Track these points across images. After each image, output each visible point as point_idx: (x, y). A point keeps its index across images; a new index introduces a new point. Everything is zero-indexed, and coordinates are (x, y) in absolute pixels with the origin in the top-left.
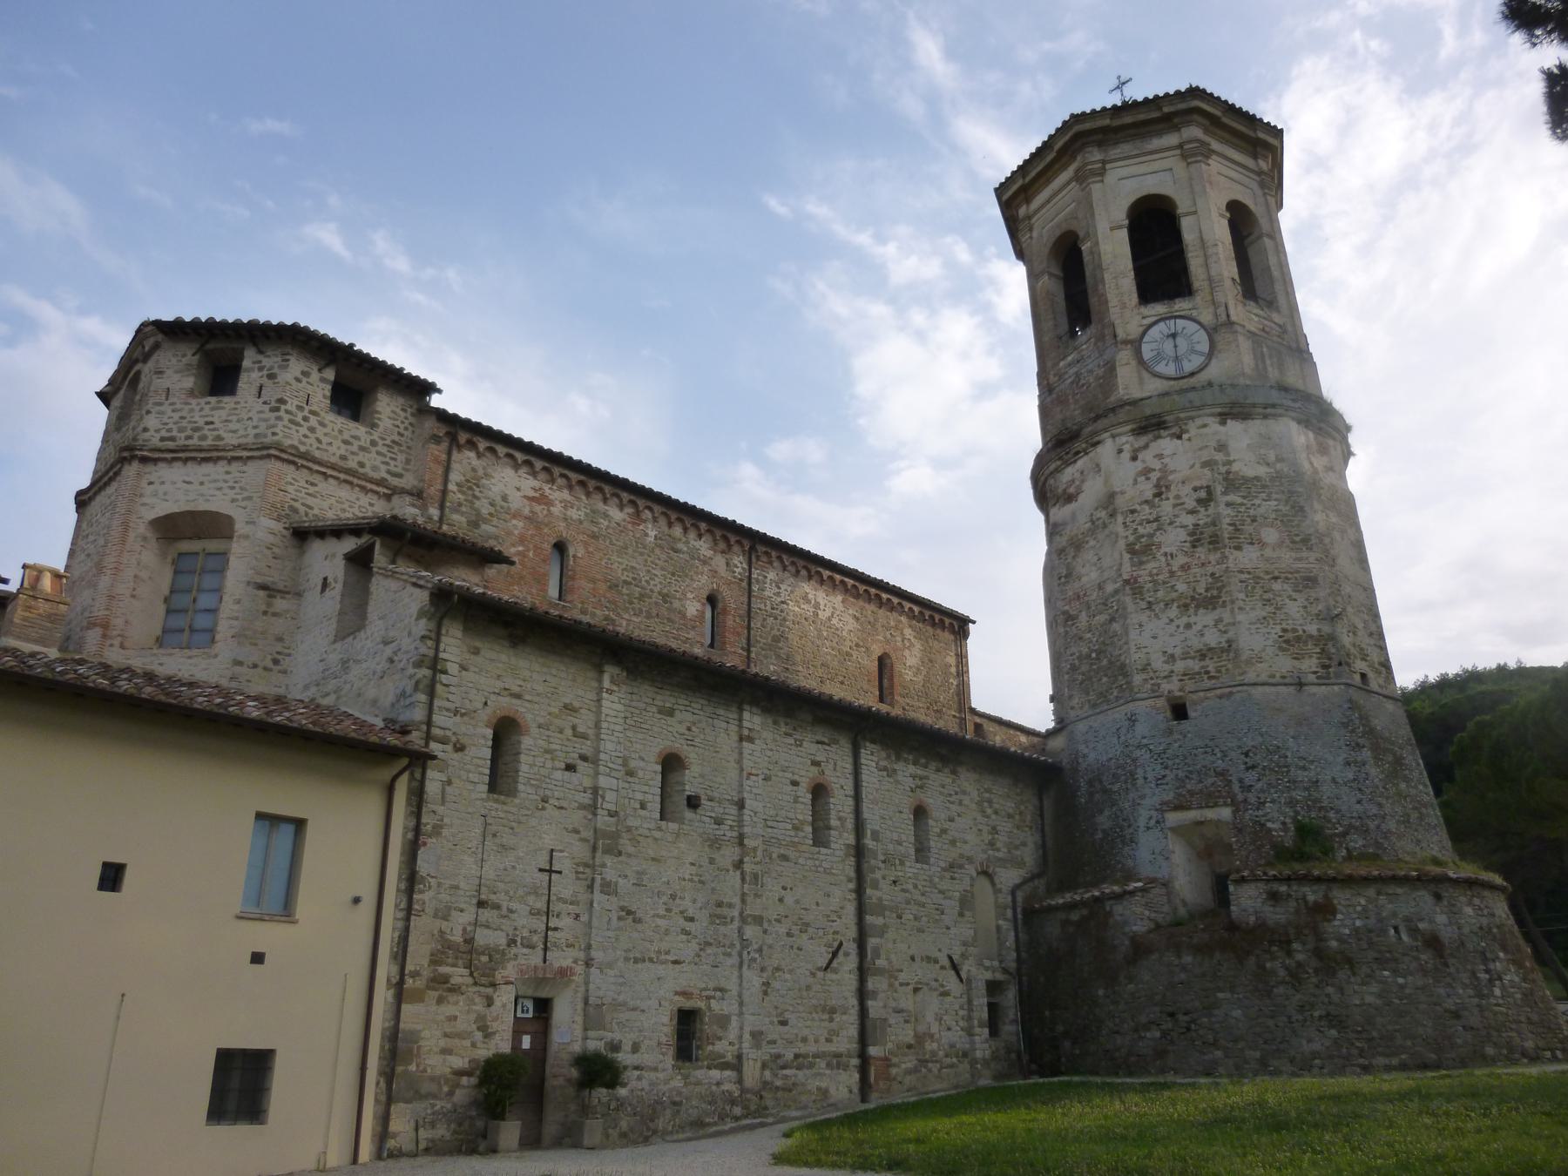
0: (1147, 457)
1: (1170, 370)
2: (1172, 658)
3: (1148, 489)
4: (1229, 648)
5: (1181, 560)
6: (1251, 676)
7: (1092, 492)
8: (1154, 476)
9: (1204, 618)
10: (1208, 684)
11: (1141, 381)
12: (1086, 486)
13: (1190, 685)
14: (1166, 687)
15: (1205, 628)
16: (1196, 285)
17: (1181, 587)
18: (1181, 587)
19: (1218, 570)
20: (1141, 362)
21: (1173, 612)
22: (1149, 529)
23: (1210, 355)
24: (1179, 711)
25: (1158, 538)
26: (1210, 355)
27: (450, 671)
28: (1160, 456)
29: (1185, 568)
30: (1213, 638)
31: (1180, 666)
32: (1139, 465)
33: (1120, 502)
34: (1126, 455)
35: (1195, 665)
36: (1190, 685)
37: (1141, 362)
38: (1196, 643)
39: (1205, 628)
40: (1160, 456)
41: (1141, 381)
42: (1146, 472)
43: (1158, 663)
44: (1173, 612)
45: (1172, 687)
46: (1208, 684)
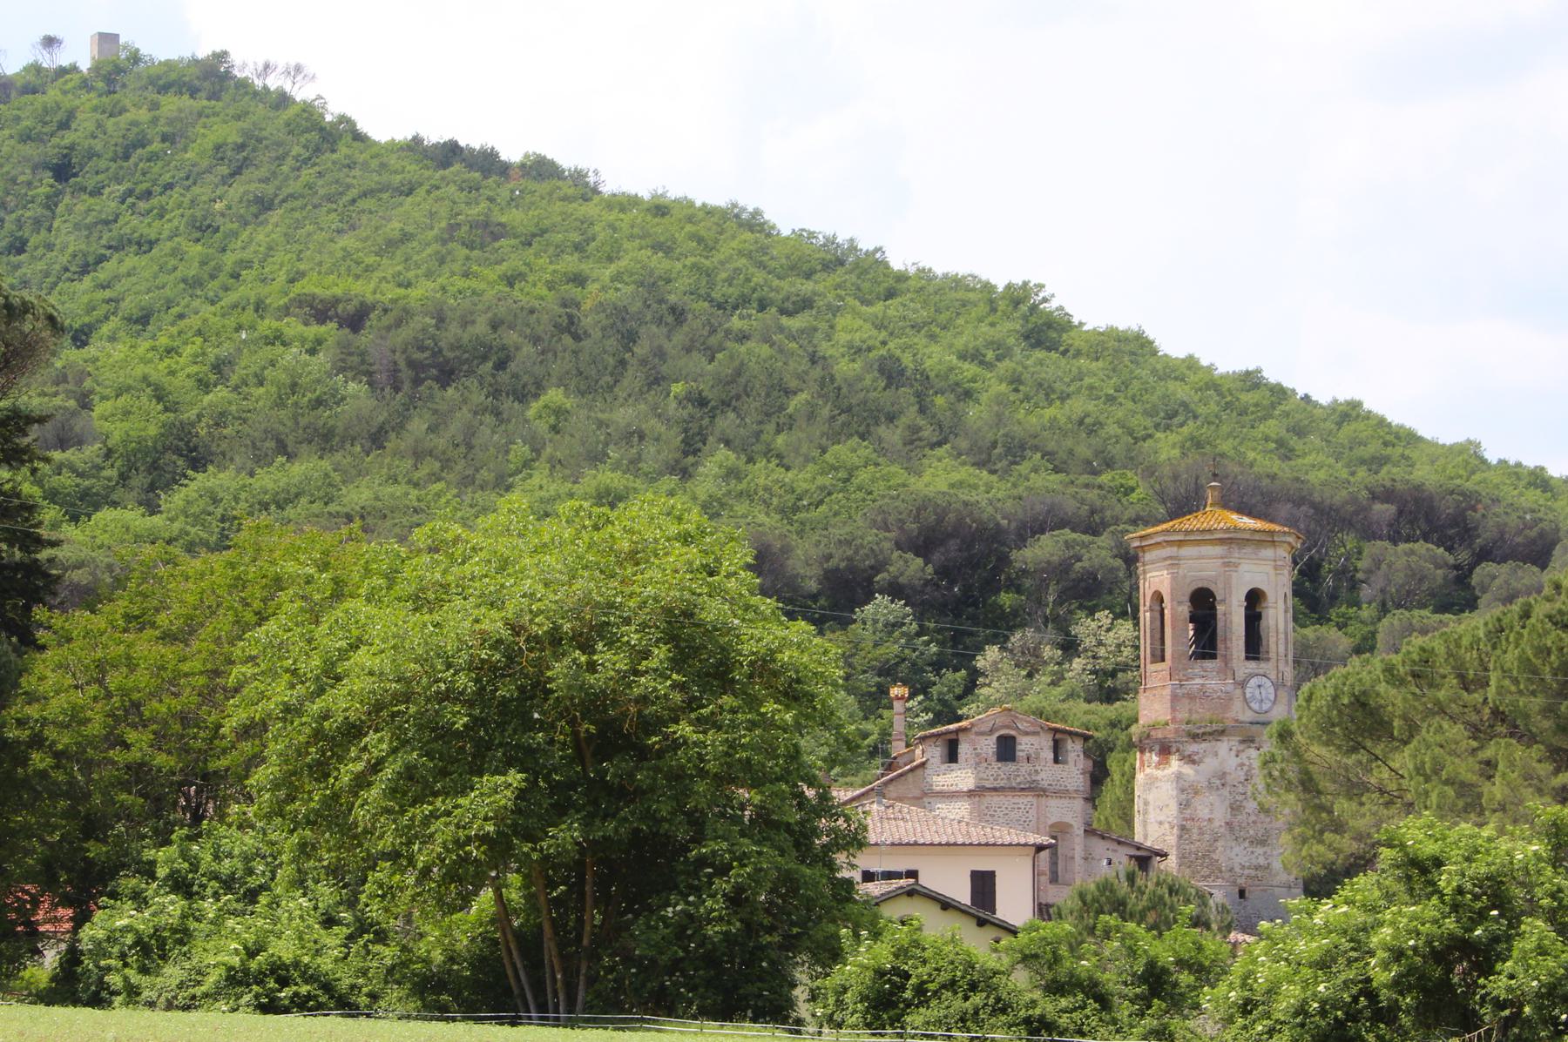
0: (1243, 756)
1: (1255, 706)
2: (1243, 867)
3: (1241, 775)
4: (1268, 867)
5: (1253, 818)
6: (1274, 883)
7: (1210, 765)
8: (1245, 768)
9: (1259, 850)
10: (1257, 882)
11: (1244, 713)
12: (1206, 760)
13: (1250, 882)
14: (1239, 881)
15: (1259, 855)
16: (1272, 655)
17: (1251, 832)
18: (1251, 832)
19: (1268, 827)
20: (1245, 699)
21: (1247, 844)
22: (1240, 798)
23: (1274, 703)
24: (1242, 894)
25: (1244, 803)
26: (1274, 703)
27: (1020, 966)
28: (1249, 758)
29: (1254, 822)
30: (1262, 861)
31: (1247, 872)
32: (1238, 760)
33: (1229, 778)
34: (1233, 753)
35: (1253, 873)
36: (1250, 882)
37: (1245, 699)
38: (1254, 862)
39: (1259, 855)
40: (1249, 758)
41: (1244, 713)
42: (1242, 765)
43: (1237, 869)
44: (1247, 844)
45: (1241, 881)
46: (1257, 882)
